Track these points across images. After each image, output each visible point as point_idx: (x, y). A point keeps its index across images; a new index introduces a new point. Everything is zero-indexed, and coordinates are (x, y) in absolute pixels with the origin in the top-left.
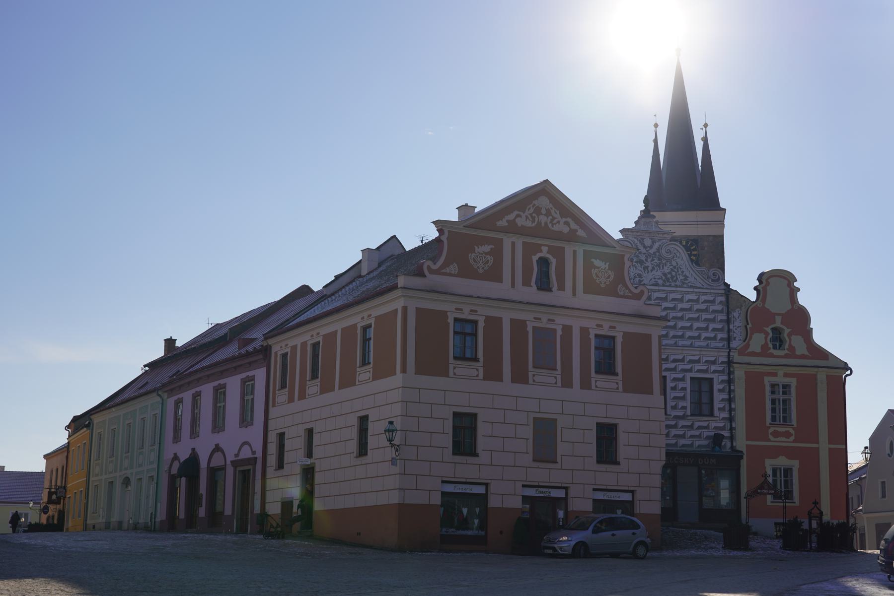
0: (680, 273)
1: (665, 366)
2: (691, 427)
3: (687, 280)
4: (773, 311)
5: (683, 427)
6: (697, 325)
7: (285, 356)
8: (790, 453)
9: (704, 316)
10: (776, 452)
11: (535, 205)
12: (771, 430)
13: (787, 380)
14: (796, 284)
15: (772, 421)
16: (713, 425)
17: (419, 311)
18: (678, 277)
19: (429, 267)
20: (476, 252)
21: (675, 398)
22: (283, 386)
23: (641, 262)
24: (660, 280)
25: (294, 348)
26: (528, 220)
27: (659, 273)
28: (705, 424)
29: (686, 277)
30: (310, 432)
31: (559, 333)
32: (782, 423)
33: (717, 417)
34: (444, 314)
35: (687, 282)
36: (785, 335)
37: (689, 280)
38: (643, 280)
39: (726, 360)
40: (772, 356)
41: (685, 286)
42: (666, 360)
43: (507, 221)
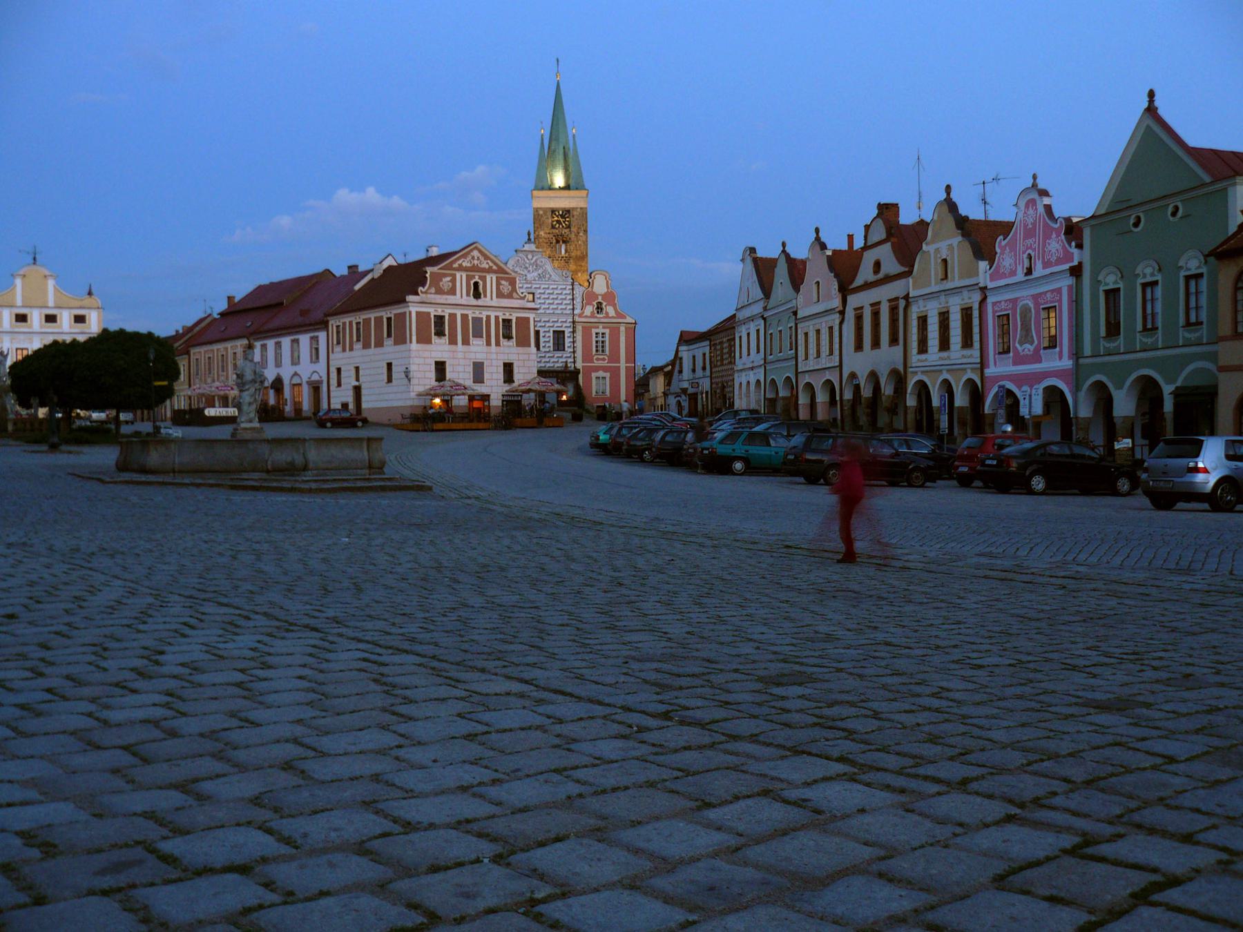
1: (539, 324)
2: (553, 357)
4: (597, 293)
6: (556, 302)
8: (605, 369)
10: (597, 369)
12: (595, 357)
13: (603, 331)
16: (565, 355)
21: (545, 342)
23: (526, 268)
27: (536, 274)
29: (551, 276)
31: (484, 319)
36: (604, 306)
40: (596, 317)
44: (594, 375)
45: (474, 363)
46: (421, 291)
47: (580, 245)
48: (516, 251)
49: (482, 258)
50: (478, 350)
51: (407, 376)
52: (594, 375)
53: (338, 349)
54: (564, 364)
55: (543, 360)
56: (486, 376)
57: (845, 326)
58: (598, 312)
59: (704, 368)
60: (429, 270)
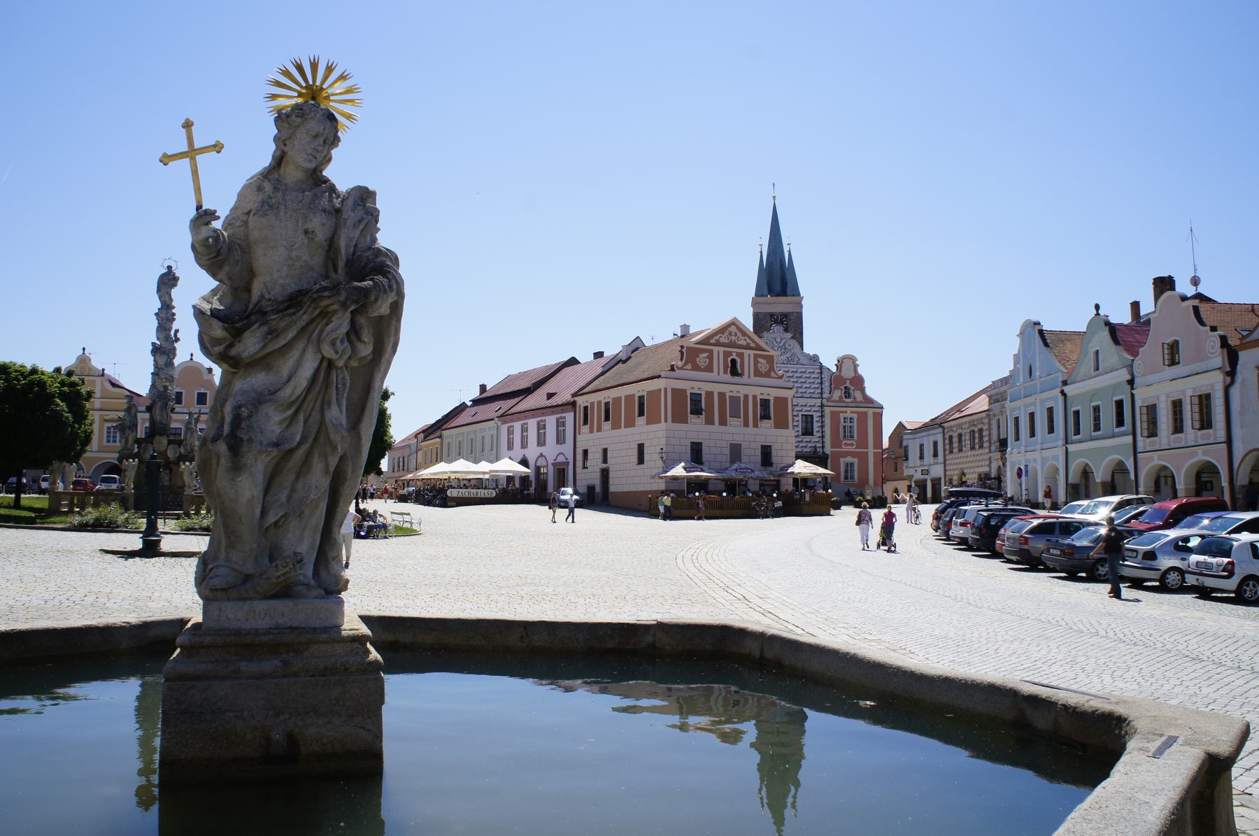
2: (802, 441)
6: (805, 385)
7: (586, 408)
9: (809, 381)
10: (846, 454)
12: (844, 442)
14: (857, 362)
16: (813, 440)
17: (673, 390)
22: (585, 422)
25: (592, 404)
27: (784, 357)
28: (809, 440)
29: (799, 359)
30: (605, 451)
31: (742, 399)
34: (685, 391)
39: (820, 404)
45: (731, 444)
49: (739, 334)
50: (735, 431)
52: (842, 460)
53: (585, 429)
54: (813, 449)
55: (801, 445)
57: (1235, 392)
59: (935, 455)
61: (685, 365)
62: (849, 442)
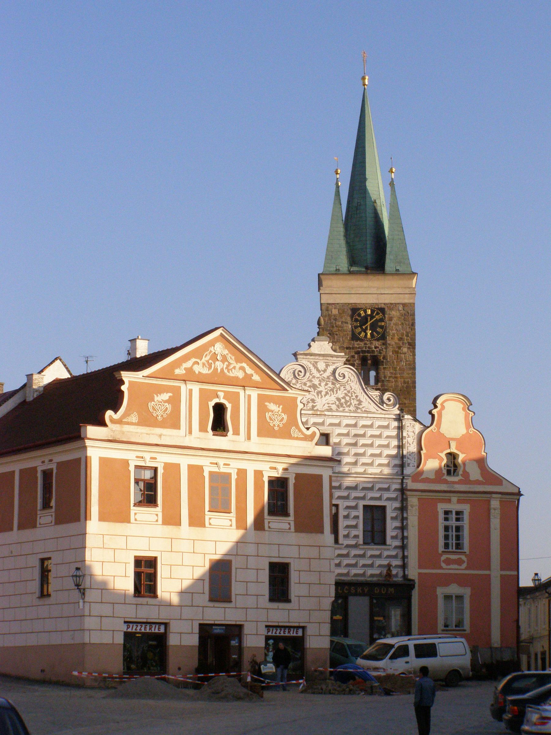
0: (354, 397)
1: (337, 493)
2: (363, 556)
3: (361, 405)
5: (355, 556)
8: (460, 580)
9: (378, 442)
11: (211, 351)
12: (444, 557)
15: (445, 549)
16: (386, 553)
18: (352, 401)
19: (110, 416)
20: (156, 401)
21: (347, 527)
23: (314, 387)
24: (334, 405)
26: (204, 366)
27: (332, 398)
28: (377, 553)
29: (360, 402)
31: (234, 477)
32: (454, 550)
33: (390, 545)
34: (126, 463)
35: (361, 407)
37: (364, 404)
38: (316, 405)
40: (446, 482)
41: (359, 411)
42: (339, 487)
43: (185, 369)
44: (441, 591)
46: (113, 421)
47: (401, 369)
48: (295, 355)
49: (231, 359)
51: (78, 585)
52: (441, 591)
54: (385, 571)
55: (346, 561)
56: (236, 588)
58: (449, 473)
60: (127, 376)
61: (126, 414)
62: (453, 557)
